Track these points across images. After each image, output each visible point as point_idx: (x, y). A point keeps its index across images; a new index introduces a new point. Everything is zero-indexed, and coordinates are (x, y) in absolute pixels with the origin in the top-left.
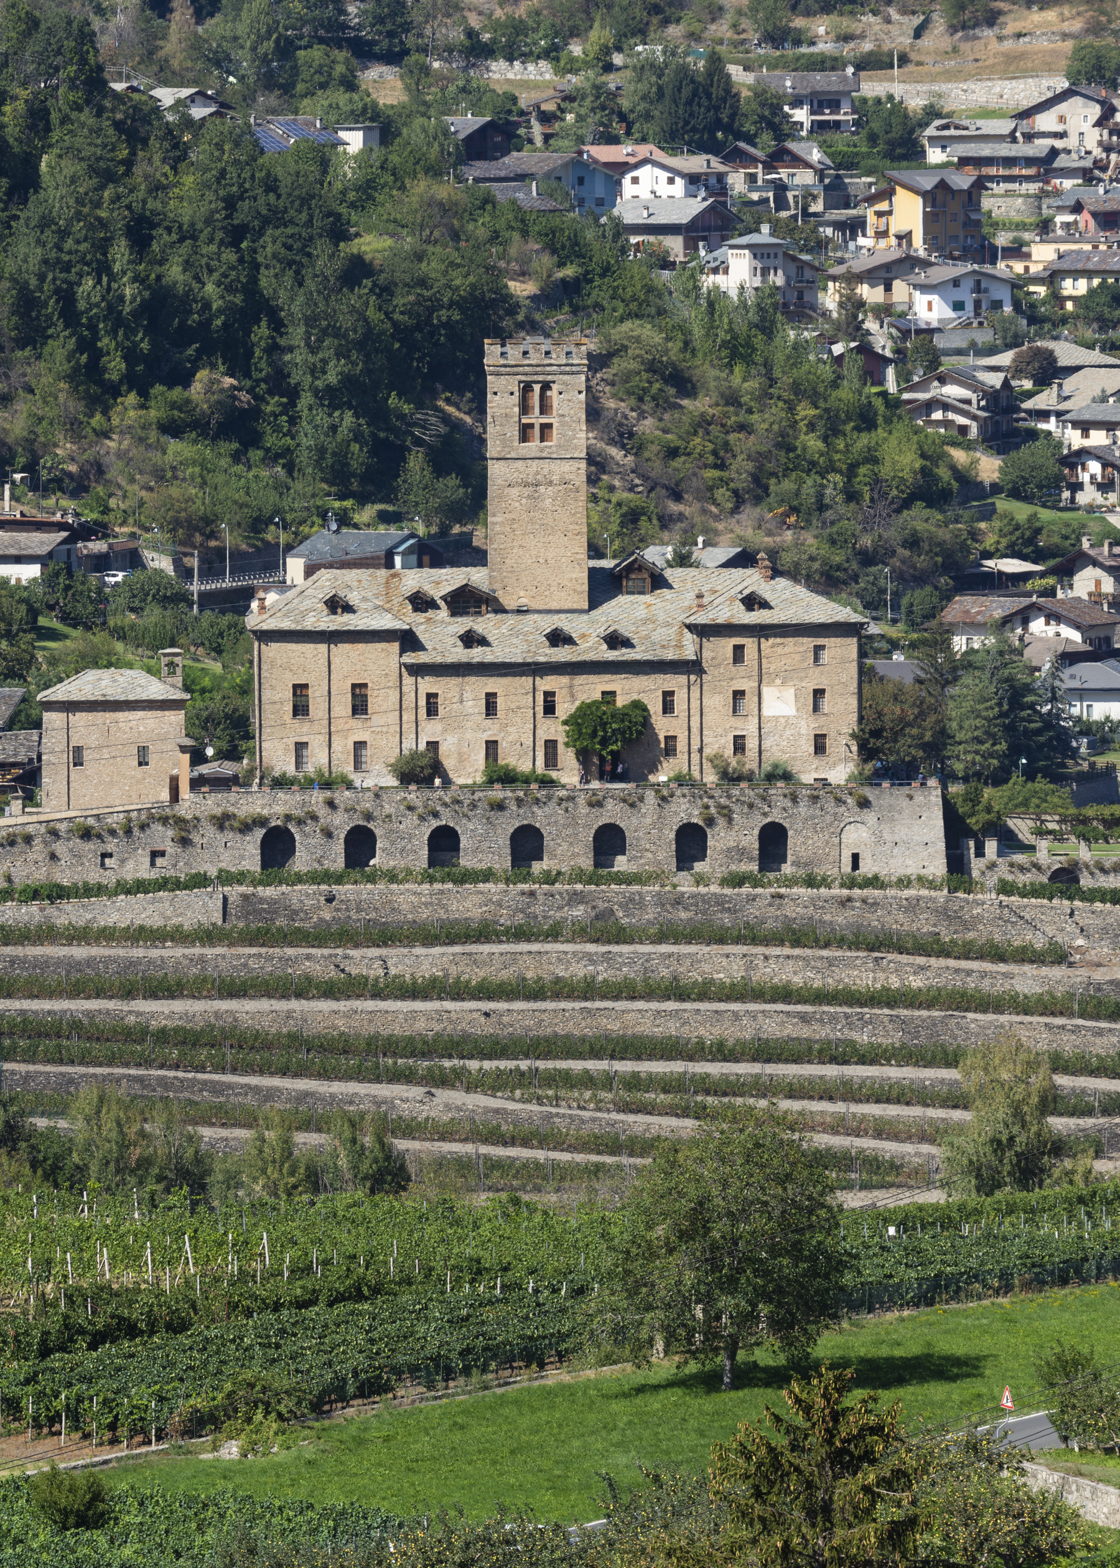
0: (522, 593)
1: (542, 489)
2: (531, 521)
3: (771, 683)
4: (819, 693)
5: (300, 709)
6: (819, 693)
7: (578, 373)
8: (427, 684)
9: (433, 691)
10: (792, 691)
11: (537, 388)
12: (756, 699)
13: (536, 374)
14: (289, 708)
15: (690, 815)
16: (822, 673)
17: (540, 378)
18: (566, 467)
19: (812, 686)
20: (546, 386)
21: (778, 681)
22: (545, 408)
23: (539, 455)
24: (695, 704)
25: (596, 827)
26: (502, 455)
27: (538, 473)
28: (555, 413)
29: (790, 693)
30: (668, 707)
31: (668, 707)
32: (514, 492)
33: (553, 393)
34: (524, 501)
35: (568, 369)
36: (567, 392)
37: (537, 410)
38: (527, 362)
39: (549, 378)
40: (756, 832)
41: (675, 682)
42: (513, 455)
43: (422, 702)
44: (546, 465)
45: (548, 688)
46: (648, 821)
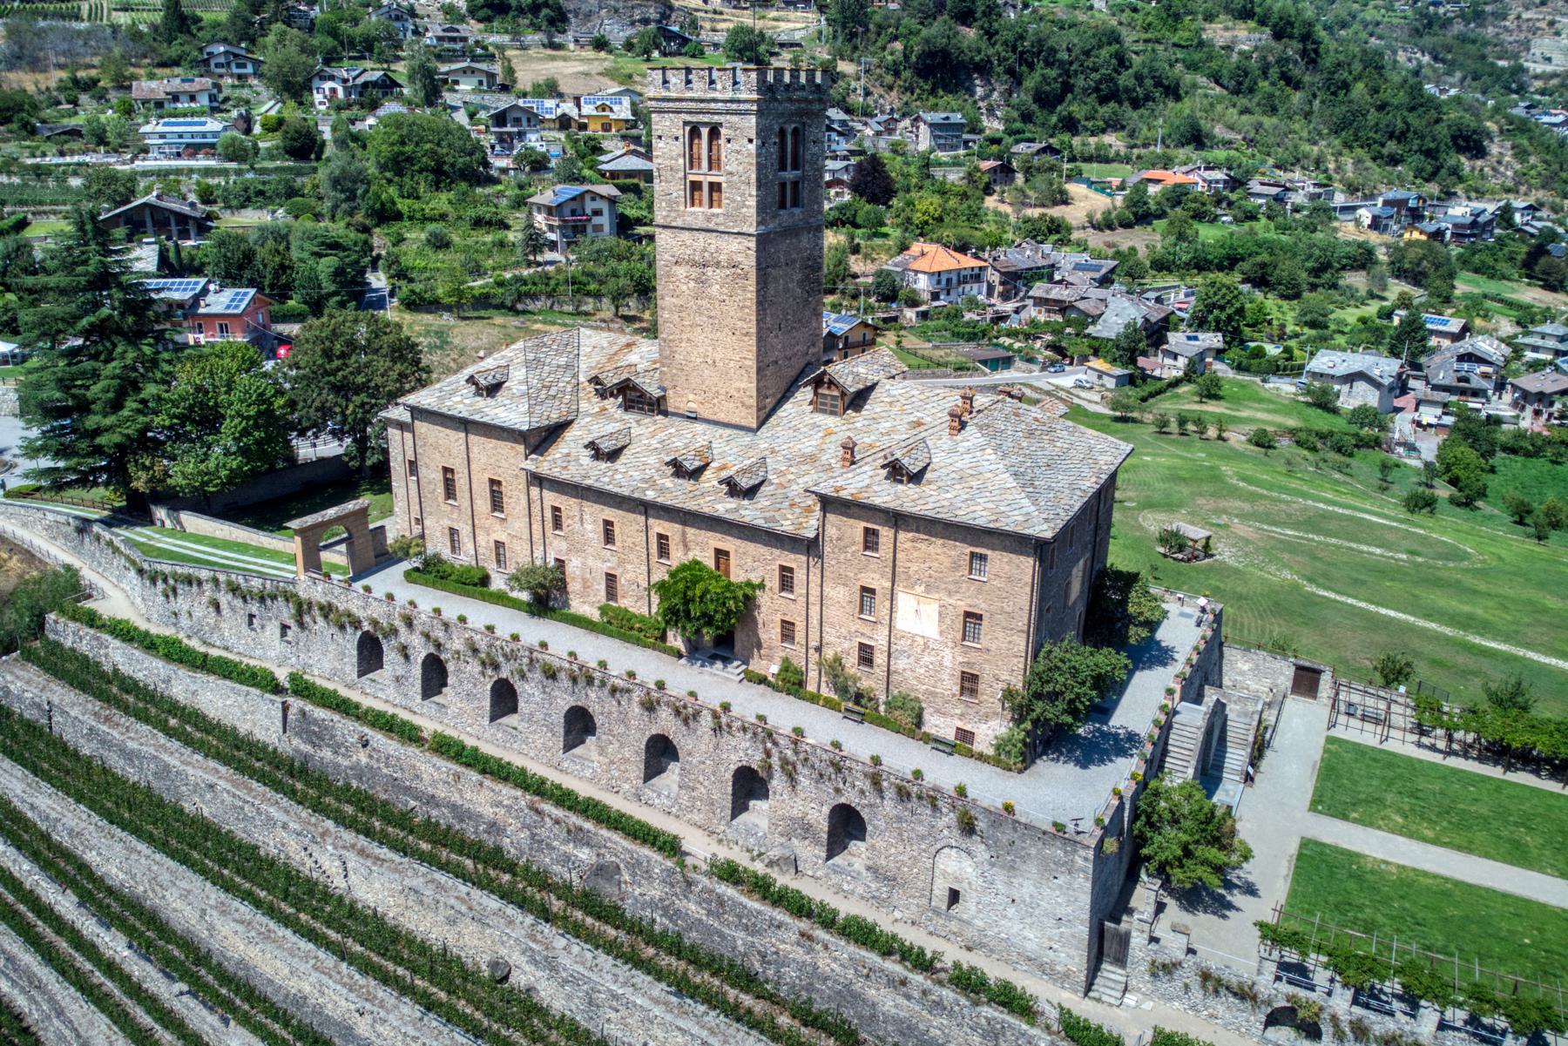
0: (691, 397)
6: (972, 617)
7: (746, 113)
10: (935, 607)
11: (705, 131)
12: (887, 604)
16: (979, 591)
17: (706, 118)
19: (964, 606)
21: (920, 589)
22: (714, 163)
29: (931, 610)
32: (681, 271)
34: (692, 284)
35: (734, 106)
37: (705, 164)
38: (689, 94)
39: (716, 118)
41: (796, 561)
42: (679, 223)
43: (548, 514)
44: (714, 242)
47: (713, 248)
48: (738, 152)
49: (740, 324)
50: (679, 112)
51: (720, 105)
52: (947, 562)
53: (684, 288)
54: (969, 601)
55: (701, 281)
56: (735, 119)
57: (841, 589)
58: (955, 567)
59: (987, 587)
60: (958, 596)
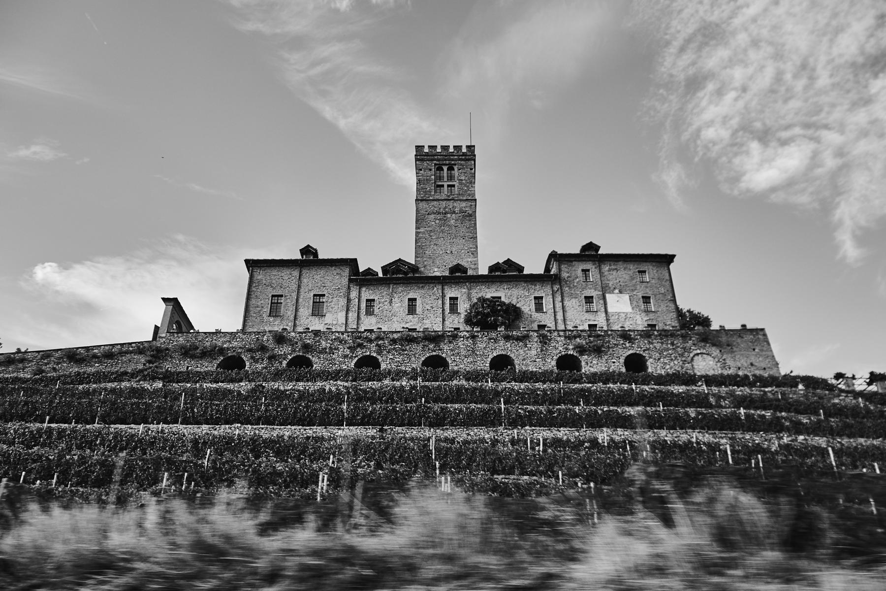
0: (436, 270)
1: (449, 215)
2: (442, 231)
3: (612, 292)
4: (646, 299)
5: (275, 310)
8: (366, 294)
9: (371, 298)
11: (445, 168)
12: (602, 302)
13: (446, 160)
14: (267, 310)
15: (567, 349)
16: (647, 287)
17: (447, 162)
18: (464, 204)
19: (640, 295)
20: (451, 168)
21: (617, 291)
22: (451, 178)
23: (447, 198)
24: (559, 305)
25: (491, 357)
26: (424, 198)
27: (446, 207)
28: (456, 179)
29: (626, 297)
30: (539, 308)
31: (539, 308)
32: (432, 216)
33: (456, 172)
34: (437, 222)
36: (464, 169)
37: (446, 179)
40: (622, 360)
41: (544, 292)
42: (431, 198)
43: (363, 305)
44: (451, 203)
45: (453, 295)
46: (534, 352)
47: (451, 207)
48: (465, 173)
49: (467, 234)
50: (432, 160)
51: (456, 157)
52: (627, 277)
53: (433, 223)
54: (643, 292)
55: (444, 220)
56: (462, 162)
57: (574, 300)
58: (632, 278)
59: (649, 285)
60: (636, 291)
